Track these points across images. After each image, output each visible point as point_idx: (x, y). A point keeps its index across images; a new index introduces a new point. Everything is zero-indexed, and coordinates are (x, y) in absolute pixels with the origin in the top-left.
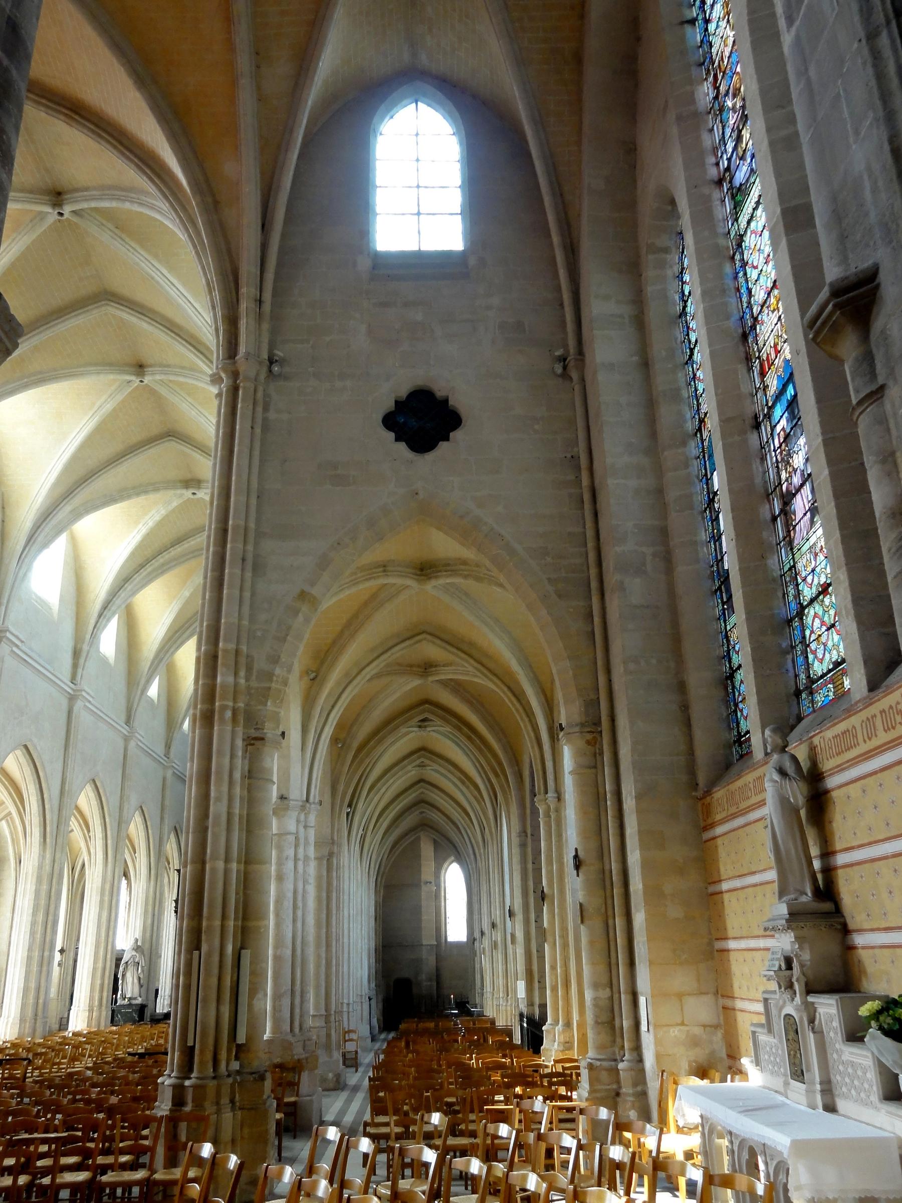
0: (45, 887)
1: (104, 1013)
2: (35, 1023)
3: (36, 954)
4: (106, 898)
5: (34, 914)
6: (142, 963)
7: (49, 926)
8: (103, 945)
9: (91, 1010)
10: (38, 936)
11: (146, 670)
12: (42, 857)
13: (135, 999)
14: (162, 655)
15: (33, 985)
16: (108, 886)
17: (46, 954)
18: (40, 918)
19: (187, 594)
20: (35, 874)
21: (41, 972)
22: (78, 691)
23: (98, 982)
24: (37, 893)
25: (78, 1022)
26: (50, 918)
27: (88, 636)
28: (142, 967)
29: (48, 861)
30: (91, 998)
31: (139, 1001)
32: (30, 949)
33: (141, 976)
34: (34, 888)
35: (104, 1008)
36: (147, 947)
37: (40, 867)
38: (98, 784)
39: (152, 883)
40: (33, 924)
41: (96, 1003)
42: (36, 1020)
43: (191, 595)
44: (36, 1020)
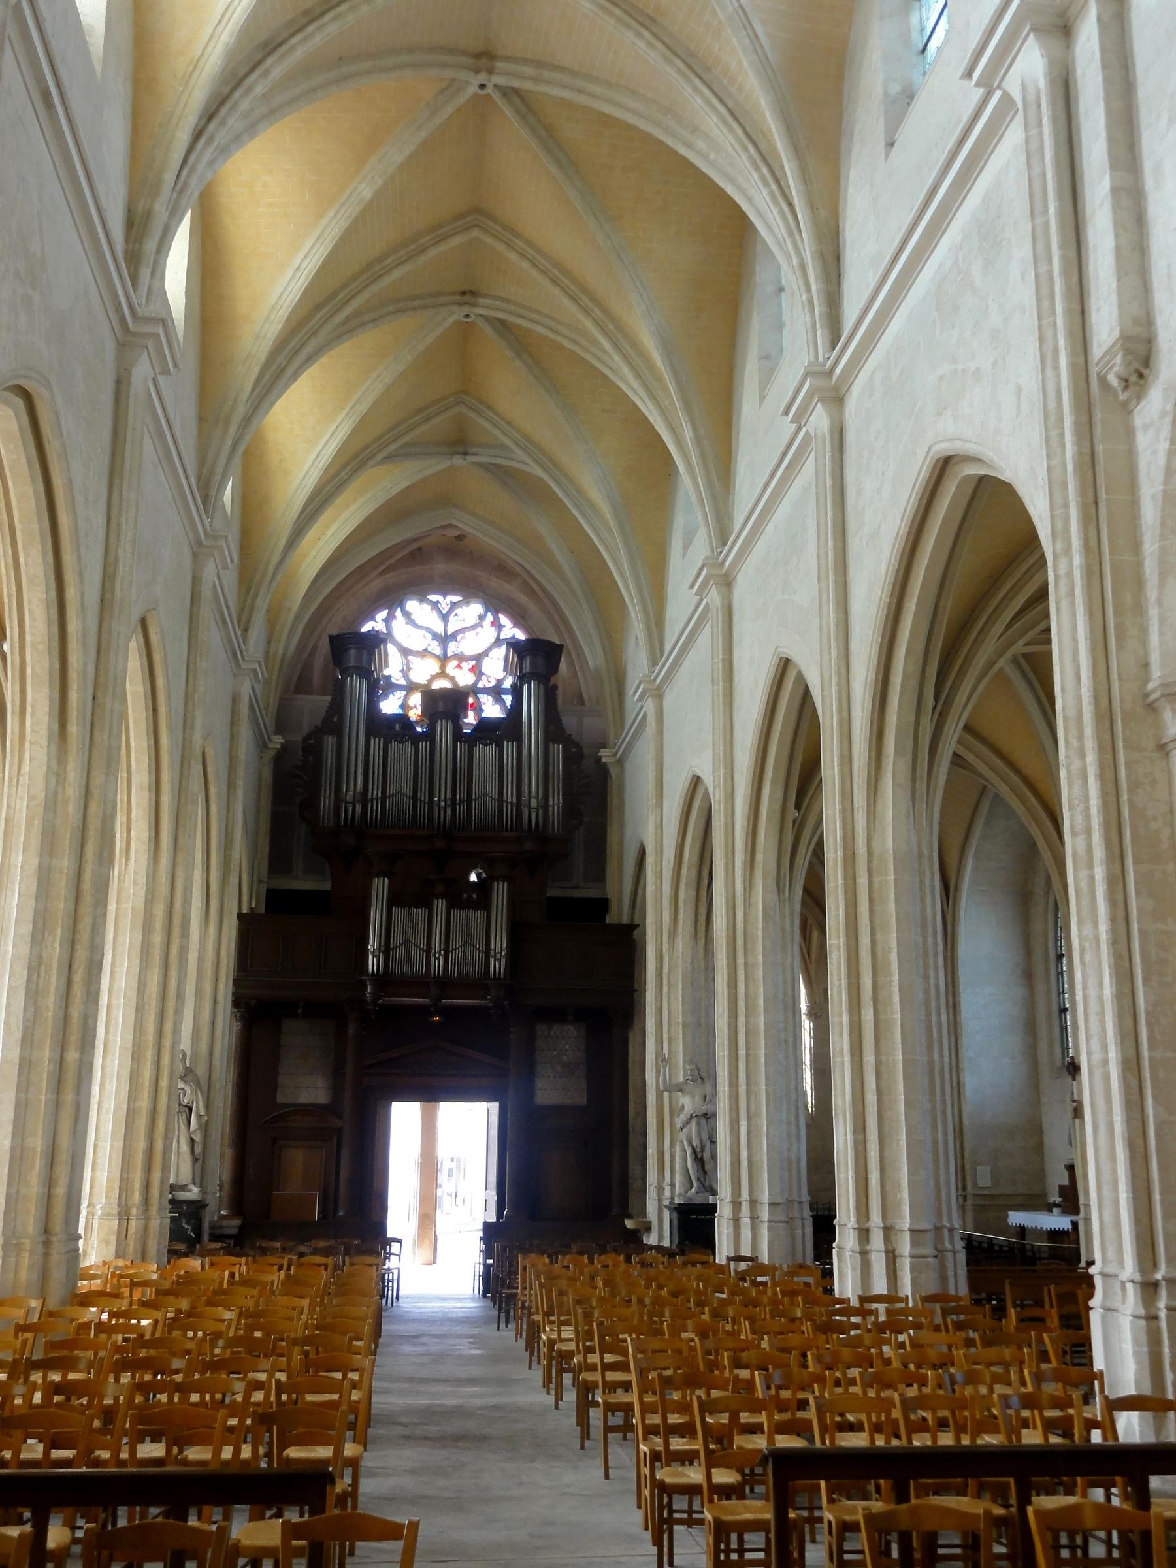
0: (65, 863)
1: (155, 1223)
2: (46, 1255)
3: (45, 1054)
4: (158, 939)
5: (38, 937)
6: (199, 1107)
7: (78, 978)
8: (149, 1055)
9: (124, 1214)
10: (51, 1002)
11: (248, 387)
12: (57, 775)
13: (183, 1188)
14: (281, 359)
15: (37, 1143)
16: (160, 911)
17: (72, 1055)
18: (55, 949)
19: (366, 191)
20: (37, 823)
21: (57, 1105)
22: (149, 320)
23: (141, 1145)
24: (44, 877)
25: (96, 1248)
26: (81, 954)
27: (169, 178)
28: (199, 1116)
29: (72, 789)
30: (125, 1185)
31: (194, 1193)
32: (28, 1040)
33: (198, 1138)
34: (34, 862)
35: (154, 1210)
36: (201, 1071)
37: (52, 804)
38: (154, 637)
39: (212, 929)
40: (36, 966)
41: (137, 1197)
42: (47, 1244)
43: (377, 194)
44: (47, 1244)
